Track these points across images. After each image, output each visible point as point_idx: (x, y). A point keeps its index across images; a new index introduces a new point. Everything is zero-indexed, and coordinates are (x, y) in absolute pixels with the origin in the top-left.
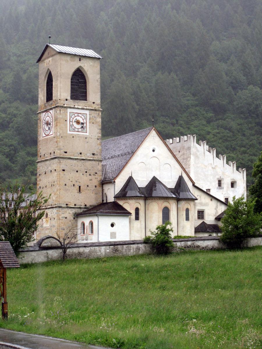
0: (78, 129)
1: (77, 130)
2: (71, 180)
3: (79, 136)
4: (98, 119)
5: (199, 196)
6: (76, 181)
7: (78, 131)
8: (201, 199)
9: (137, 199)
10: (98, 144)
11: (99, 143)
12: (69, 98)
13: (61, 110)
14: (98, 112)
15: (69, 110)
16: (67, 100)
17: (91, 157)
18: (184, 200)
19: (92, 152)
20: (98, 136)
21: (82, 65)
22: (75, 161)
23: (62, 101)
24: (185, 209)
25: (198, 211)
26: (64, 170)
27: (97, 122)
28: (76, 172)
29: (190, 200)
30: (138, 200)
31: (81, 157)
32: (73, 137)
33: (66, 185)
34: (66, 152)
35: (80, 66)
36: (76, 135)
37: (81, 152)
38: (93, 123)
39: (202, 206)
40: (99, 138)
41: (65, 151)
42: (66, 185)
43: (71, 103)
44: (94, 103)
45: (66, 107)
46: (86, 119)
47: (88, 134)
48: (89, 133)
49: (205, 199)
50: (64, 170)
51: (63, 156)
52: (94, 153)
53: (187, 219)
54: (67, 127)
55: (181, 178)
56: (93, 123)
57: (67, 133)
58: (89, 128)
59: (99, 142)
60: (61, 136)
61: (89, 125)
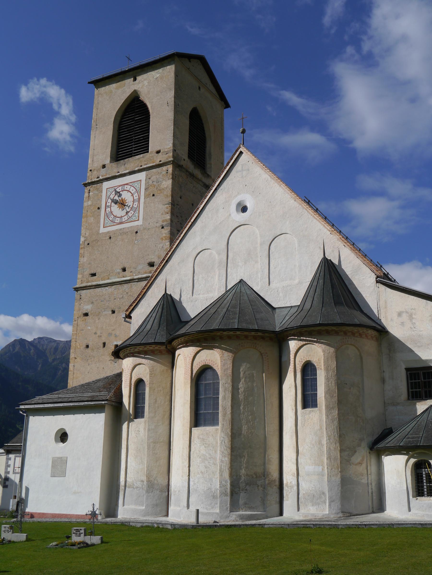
0: (122, 217)
1: (118, 220)
2: (99, 333)
3: (123, 232)
4: (164, 183)
5: (404, 315)
7: (121, 223)
10: (162, 239)
11: (164, 235)
12: (107, 161)
13: (91, 189)
14: (164, 168)
15: (106, 185)
16: (104, 166)
17: (146, 273)
19: (149, 261)
20: (163, 221)
21: (136, 89)
23: (95, 172)
25: (407, 370)
26: (86, 315)
28: (111, 312)
31: (124, 277)
32: (110, 238)
33: (87, 346)
34: (94, 275)
35: (135, 92)
36: (114, 232)
37: (127, 266)
38: (153, 195)
40: (164, 224)
41: (93, 272)
42: (87, 346)
43: (114, 169)
44: (158, 152)
45: (101, 181)
46: (138, 192)
50: (86, 315)
51: (89, 284)
52: (153, 260)
54: (99, 222)
56: (153, 195)
57: (98, 233)
59: (165, 233)
60: (86, 243)
61: (145, 203)
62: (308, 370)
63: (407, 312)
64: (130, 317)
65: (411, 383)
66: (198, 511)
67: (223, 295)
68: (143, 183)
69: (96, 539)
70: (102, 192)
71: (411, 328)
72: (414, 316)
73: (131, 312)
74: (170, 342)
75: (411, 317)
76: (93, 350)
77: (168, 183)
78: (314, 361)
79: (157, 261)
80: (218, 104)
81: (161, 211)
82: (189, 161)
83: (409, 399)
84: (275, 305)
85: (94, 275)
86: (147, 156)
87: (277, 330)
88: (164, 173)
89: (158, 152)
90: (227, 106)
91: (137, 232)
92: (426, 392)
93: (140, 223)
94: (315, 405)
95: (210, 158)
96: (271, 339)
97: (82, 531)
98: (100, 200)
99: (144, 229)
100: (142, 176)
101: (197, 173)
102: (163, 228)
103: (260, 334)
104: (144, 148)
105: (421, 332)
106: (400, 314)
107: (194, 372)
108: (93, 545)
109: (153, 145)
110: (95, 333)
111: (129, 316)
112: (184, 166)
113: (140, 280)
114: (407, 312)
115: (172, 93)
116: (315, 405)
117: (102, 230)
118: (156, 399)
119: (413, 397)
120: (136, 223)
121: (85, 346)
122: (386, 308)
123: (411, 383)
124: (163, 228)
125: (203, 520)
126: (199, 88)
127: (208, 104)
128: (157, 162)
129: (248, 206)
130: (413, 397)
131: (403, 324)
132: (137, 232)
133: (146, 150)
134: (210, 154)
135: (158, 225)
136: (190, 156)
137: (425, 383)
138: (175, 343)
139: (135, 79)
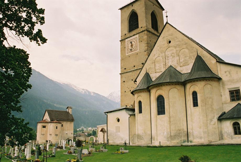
3: (133, 55)
5: (227, 73)
6: (132, 87)
8: (231, 75)
9: (139, 92)
10: (145, 55)
14: (144, 32)
15: (126, 40)
18: (189, 83)
22: (130, 73)
24: (191, 93)
26: (124, 82)
27: (143, 40)
29: (197, 81)
30: (139, 94)
34: (125, 69)
35: (133, 9)
36: (130, 55)
39: (233, 83)
41: (125, 68)
42: (125, 92)
44: (142, 27)
45: (125, 39)
47: (138, 50)
48: (139, 49)
49: (237, 73)
50: (124, 82)
52: (143, 62)
53: (195, 104)
55: (199, 59)
58: (139, 45)
62: (195, 94)
63: (228, 71)
64: (136, 81)
65: (231, 96)
66: (160, 142)
67: (165, 71)
68: (138, 38)
69: (127, 151)
70: (125, 43)
71: (230, 77)
72: (231, 72)
73: (136, 80)
74: (148, 88)
75: (230, 73)
76: (127, 93)
77: (145, 37)
78: (196, 90)
79: (144, 62)
80: (160, 10)
81: (144, 46)
82: (152, 29)
83: (231, 101)
84: (182, 73)
85: (125, 69)
86: (138, 29)
87: (183, 81)
88: (144, 34)
89: (142, 27)
90: (164, 10)
91: (137, 54)
92: (237, 98)
93: (138, 50)
94: (197, 106)
95: (159, 27)
96: (181, 84)
97: (123, 149)
98: (125, 45)
99: (139, 52)
100: (137, 36)
101: (156, 33)
102: (145, 51)
103: (177, 83)
104: (137, 27)
105: (234, 78)
106: (226, 72)
107: (156, 97)
108: (126, 153)
109: (140, 26)
110: (127, 87)
111: (136, 81)
112: (151, 31)
113: (139, 69)
114: (228, 71)
115: (144, 8)
116: (197, 106)
117: (127, 54)
118: (145, 107)
119: (232, 101)
120: (137, 51)
121: (124, 92)
122: (220, 70)
123: (231, 96)
124: (145, 51)
125: (161, 145)
126: (153, 5)
127: (157, 10)
128: (142, 31)
129: (171, 41)
130: (232, 101)
131: (227, 75)
132: (137, 54)
133: (138, 27)
134: (159, 26)
135: (144, 51)
136: (152, 27)
137: (236, 95)
138: (150, 88)
139: (132, 6)
